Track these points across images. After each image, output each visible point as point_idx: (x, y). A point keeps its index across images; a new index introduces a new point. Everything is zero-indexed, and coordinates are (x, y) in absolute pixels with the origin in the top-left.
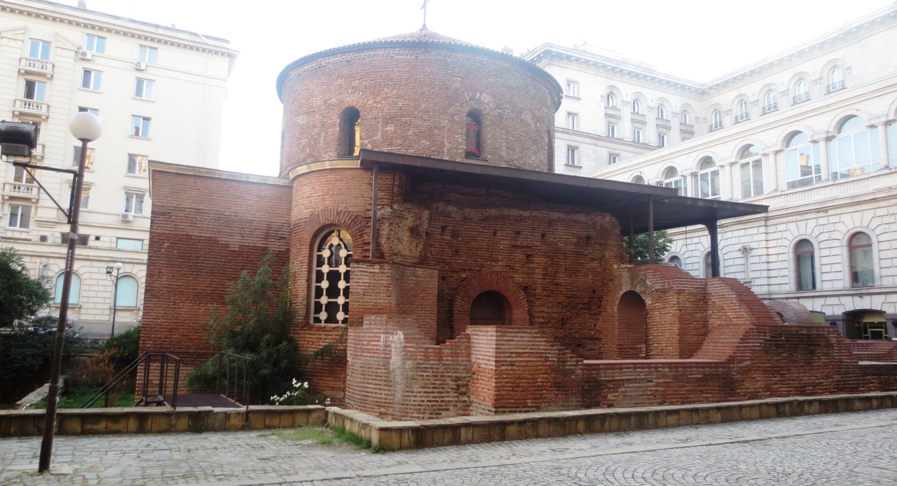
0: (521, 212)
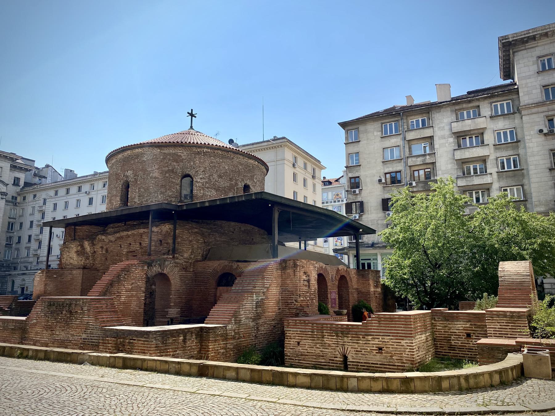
0: (127, 233)
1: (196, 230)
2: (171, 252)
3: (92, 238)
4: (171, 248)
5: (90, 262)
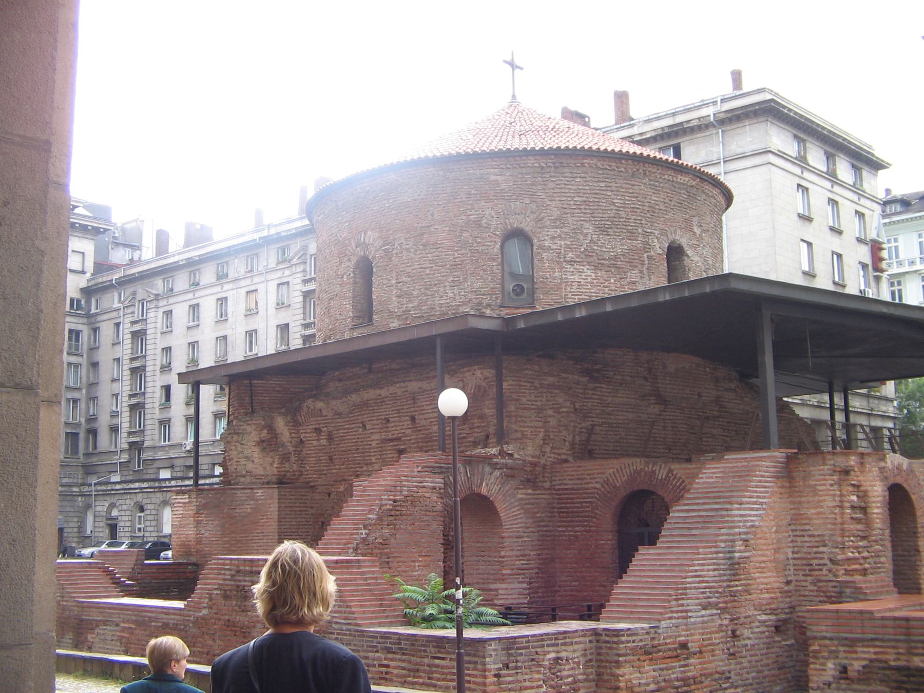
0: (378, 392)
1: (551, 380)
2: (492, 440)
3: (291, 406)
4: (492, 430)
5: (292, 466)
